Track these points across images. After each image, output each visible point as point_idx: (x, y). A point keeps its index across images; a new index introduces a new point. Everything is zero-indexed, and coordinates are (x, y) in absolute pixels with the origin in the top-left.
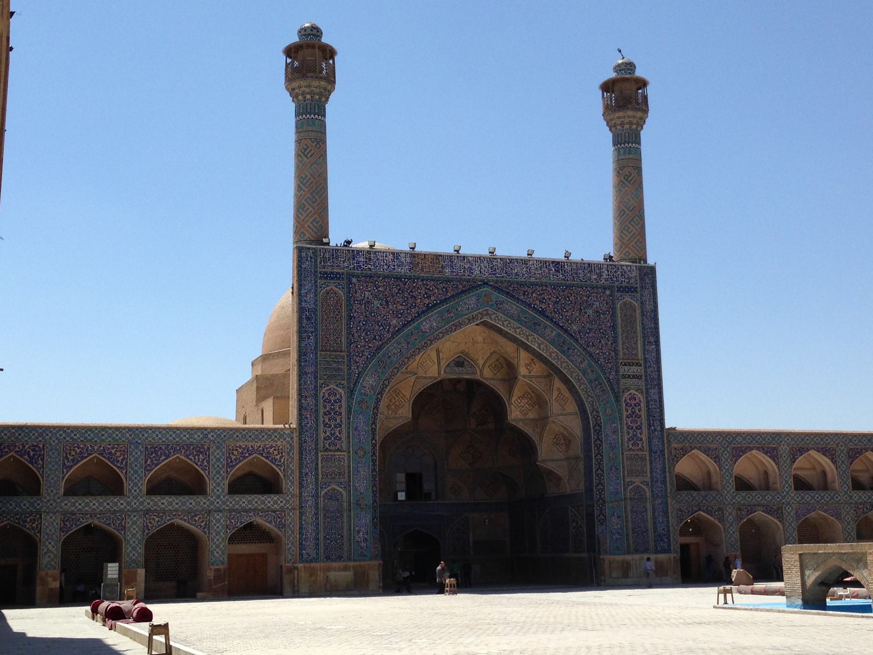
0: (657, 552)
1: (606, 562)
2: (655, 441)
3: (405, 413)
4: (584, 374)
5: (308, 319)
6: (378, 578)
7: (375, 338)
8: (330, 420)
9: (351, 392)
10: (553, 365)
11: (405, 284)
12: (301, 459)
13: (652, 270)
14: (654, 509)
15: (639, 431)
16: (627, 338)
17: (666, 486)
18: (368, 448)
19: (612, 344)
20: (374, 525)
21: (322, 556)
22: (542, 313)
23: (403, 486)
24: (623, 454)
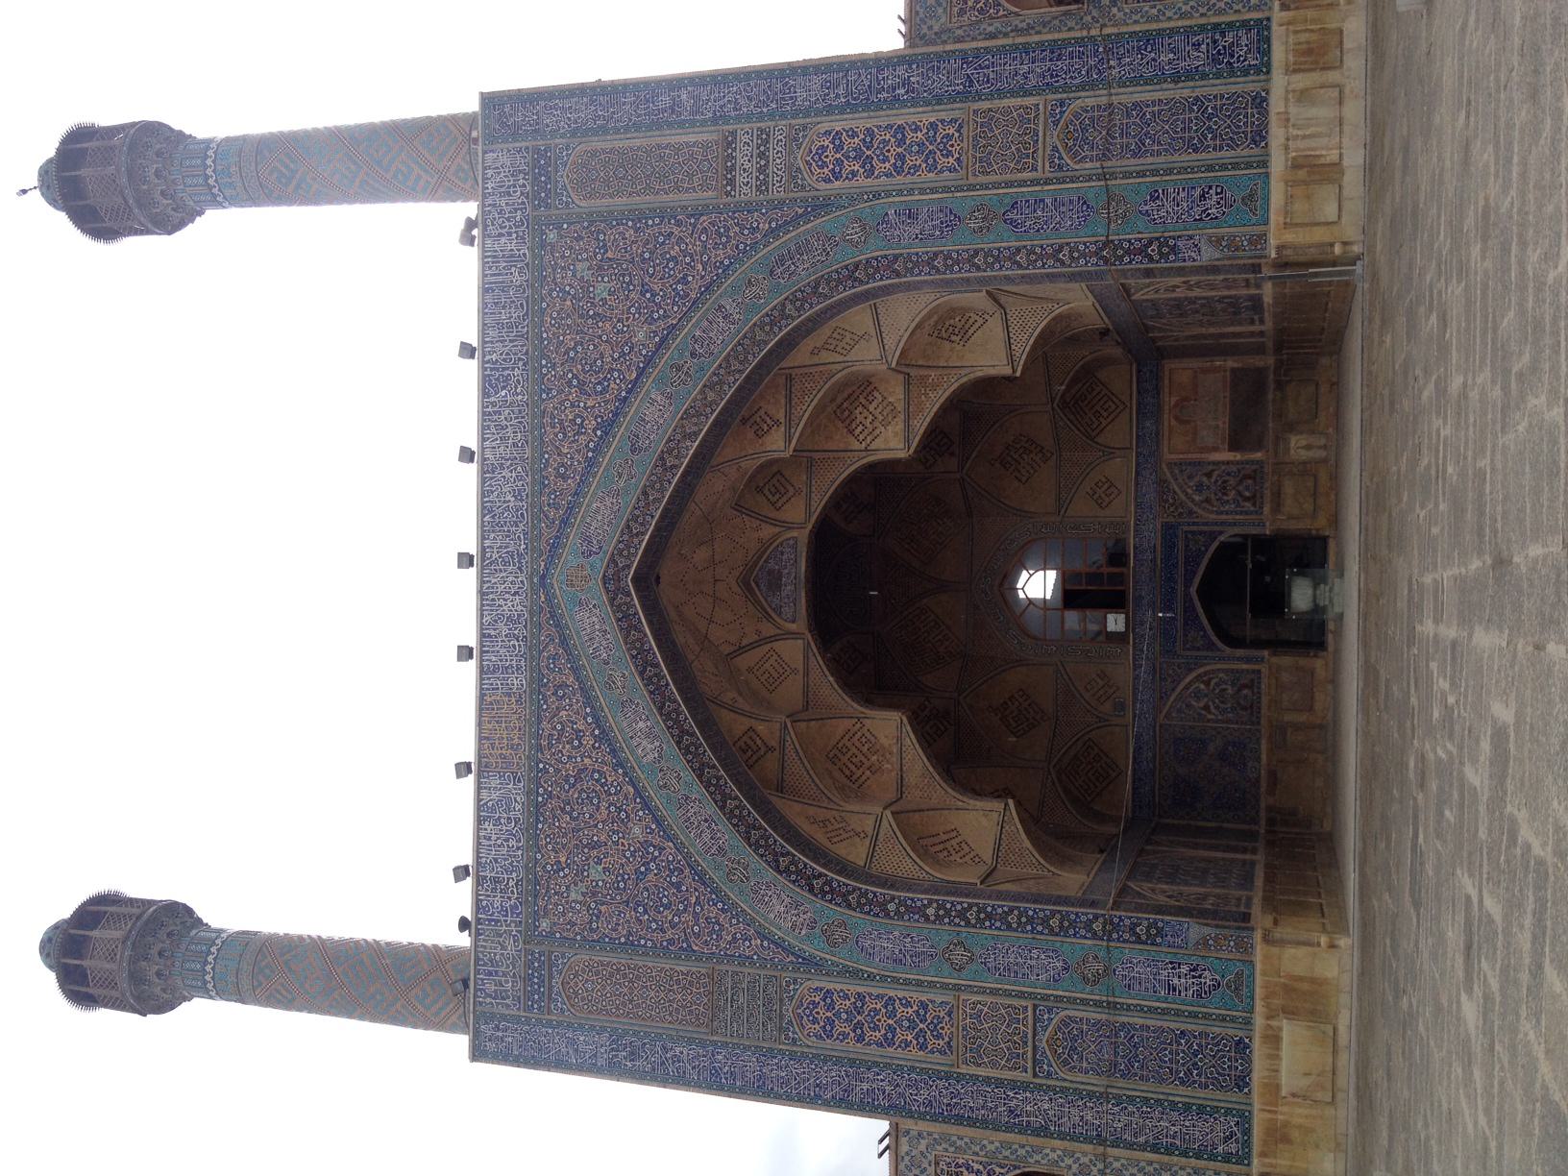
0: (1265, 68)
1: (1289, 237)
3: (889, 729)
5: (633, 1056)
6: (1301, 951)
7: (678, 886)
8: (876, 1028)
9: (811, 964)
11: (550, 795)
12: (972, 1123)
14: (1135, 81)
15: (910, 135)
17: (1067, 43)
18: (944, 934)
19: (679, 224)
21: (1234, 1097)
22: (607, 427)
23: (1098, 614)
24: (972, 187)
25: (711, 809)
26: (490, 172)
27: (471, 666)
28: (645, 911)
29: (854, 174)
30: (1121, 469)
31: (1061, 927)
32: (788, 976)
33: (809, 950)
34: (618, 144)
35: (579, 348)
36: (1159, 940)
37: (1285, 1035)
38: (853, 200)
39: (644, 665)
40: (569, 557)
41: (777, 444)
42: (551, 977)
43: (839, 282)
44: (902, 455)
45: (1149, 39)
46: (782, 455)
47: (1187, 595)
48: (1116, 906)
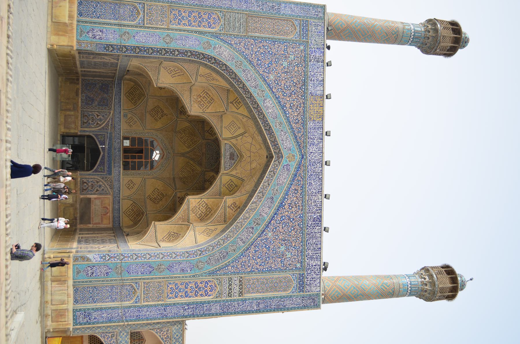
0: (75, 311)
2: (174, 310)
3: (194, 109)
4: (234, 242)
6: (62, 43)
9: (216, 36)
10: (238, 218)
13: (317, 306)
14: (114, 308)
15: (184, 294)
16: (263, 283)
17: (135, 321)
18: (173, 46)
19: (257, 269)
20: (108, 46)
22: (281, 205)
25: (247, 84)
26: (318, 285)
27: (326, 130)
28: (269, 52)
29: (201, 283)
30: (125, 192)
31: (135, 49)
32: (222, 32)
33: (216, 40)
34: (277, 293)
35: (290, 230)
36: (105, 46)
37: (67, 18)
38: (202, 275)
39: (269, 130)
40: (293, 165)
41: (229, 200)
42: (300, 31)
43: (206, 250)
44: (190, 197)
45: (110, 321)
46: (227, 197)
47: (104, 152)
48: (119, 56)
